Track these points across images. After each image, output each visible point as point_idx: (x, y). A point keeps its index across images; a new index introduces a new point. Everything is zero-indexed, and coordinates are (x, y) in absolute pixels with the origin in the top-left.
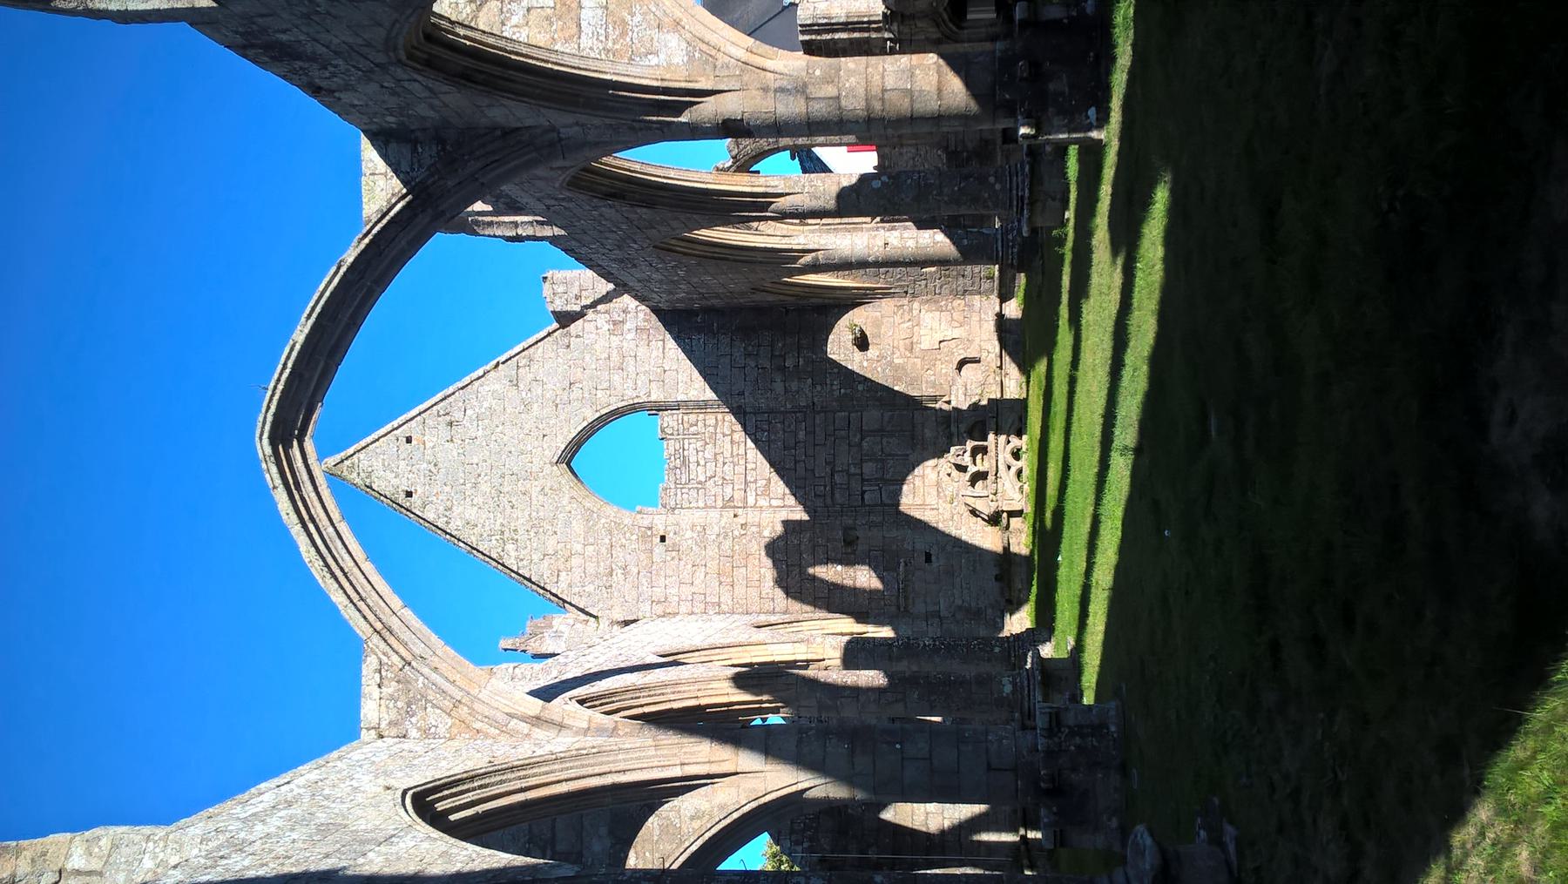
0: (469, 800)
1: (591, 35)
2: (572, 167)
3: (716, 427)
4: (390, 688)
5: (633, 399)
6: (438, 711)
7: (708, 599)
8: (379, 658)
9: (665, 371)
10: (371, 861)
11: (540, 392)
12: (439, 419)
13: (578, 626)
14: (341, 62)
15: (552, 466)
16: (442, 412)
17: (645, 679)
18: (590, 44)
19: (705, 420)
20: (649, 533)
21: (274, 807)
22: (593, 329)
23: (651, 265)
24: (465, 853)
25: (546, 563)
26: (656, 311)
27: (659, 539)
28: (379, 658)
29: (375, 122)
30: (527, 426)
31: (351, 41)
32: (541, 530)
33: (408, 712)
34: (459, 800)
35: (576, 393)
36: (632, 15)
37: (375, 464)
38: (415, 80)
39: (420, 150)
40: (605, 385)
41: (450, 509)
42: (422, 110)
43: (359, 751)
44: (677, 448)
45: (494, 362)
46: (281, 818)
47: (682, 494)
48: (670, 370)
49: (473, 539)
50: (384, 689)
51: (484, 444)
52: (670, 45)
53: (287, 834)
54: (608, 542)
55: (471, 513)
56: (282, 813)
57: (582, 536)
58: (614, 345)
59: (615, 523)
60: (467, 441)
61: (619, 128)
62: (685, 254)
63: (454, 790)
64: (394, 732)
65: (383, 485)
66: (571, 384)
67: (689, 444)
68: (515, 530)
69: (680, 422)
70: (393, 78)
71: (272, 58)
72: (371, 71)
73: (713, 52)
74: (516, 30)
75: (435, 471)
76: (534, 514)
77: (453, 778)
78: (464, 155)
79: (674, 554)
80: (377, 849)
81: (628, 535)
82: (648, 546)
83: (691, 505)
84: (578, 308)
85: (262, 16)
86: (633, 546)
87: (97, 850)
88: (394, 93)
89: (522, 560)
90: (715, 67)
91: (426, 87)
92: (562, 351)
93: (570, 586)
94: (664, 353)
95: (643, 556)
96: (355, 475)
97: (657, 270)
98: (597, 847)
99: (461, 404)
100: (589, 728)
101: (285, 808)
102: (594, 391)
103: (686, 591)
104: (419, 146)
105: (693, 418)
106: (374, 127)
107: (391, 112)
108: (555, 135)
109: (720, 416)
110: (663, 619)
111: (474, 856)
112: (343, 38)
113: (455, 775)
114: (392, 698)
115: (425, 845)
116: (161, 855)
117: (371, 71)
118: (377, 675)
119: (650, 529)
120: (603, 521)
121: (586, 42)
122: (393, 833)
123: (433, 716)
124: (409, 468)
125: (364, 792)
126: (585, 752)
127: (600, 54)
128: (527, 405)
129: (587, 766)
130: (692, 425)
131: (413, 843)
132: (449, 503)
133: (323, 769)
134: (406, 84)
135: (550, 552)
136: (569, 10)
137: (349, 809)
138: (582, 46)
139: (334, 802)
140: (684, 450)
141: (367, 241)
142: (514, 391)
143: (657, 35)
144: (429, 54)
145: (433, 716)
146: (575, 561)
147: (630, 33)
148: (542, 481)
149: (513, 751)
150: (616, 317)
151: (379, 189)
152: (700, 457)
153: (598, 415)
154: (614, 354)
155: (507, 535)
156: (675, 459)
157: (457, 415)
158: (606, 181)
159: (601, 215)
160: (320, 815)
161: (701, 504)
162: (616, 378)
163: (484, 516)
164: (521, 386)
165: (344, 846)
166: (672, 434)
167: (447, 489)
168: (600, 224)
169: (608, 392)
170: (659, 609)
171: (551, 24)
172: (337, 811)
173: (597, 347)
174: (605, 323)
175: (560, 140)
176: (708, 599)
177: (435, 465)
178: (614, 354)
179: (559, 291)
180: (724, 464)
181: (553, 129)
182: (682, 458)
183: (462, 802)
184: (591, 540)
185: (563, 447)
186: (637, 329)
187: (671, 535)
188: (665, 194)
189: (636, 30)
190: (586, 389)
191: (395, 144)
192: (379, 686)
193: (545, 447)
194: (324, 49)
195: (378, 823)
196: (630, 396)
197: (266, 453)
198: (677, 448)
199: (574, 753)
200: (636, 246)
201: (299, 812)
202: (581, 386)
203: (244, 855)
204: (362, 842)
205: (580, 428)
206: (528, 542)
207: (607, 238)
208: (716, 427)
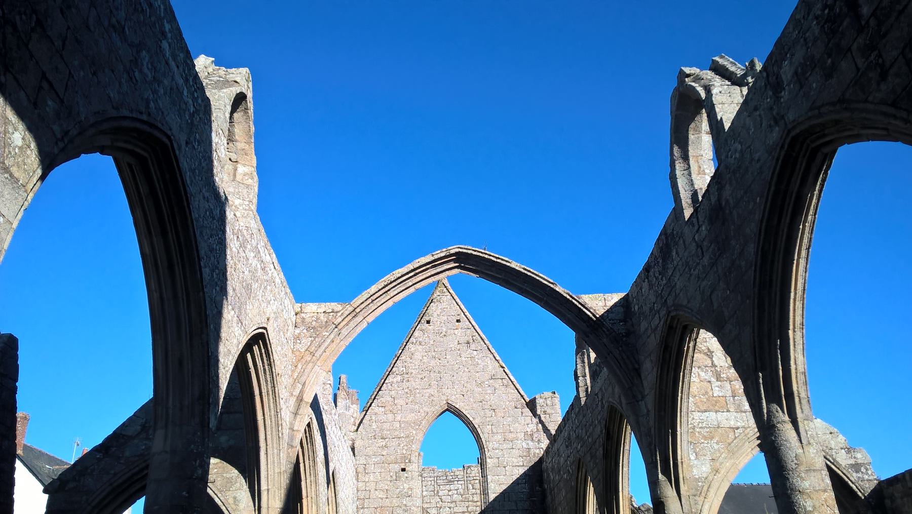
0: (258, 363)
1: (701, 418)
2: (622, 408)
3: (473, 501)
4: (323, 318)
5: (487, 448)
6: (309, 344)
7: (366, 500)
8: (340, 311)
9: (505, 467)
10: (229, 313)
11: (489, 392)
12: (471, 337)
13: (352, 420)
14: (664, 282)
15: (446, 400)
16: (474, 338)
17: (320, 463)
18: (696, 418)
19: (476, 494)
20: (407, 461)
21: (262, 261)
23: (569, 457)
24: (229, 363)
25: (390, 399)
26: (541, 461)
27: (403, 467)
28: (340, 311)
29: (633, 300)
31: (677, 287)
32: (408, 395)
33: (309, 328)
34: (258, 358)
35: (489, 413)
36: (717, 443)
37: (445, 304)
38: (660, 321)
39: (621, 324)
40: (494, 430)
41: (420, 344)
42: (644, 325)
43: (289, 303)
44: (459, 477)
45: (504, 366)
46: (256, 265)
47: (431, 481)
48: (506, 470)
49: (403, 358)
50: (323, 314)
51: (458, 361)
52: (703, 466)
53: (248, 269)
54: (402, 436)
55: (418, 356)
56: (259, 266)
57: (405, 420)
58: (519, 435)
59: (413, 440)
60: (459, 352)
61: (649, 436)
62: (577, 478)
63: (264, 355)
64: (299, 321)
67: (461, 485)
68: (408, 381)
69: (475, 478)
70: (660, 309)
71: (662, 247)
72: (662, 297)
73: (703, 494)
74: (697, 374)
75: (441, 335)
76: (418, 391)
77: (271, 354)
78: (621, 347)
79: (394, 477)
80: (236, 316)
81: (406, 448)
82: (399, 461)
83: (424, 487)
84: (539, 412)
85: (684, 242)
86: (399, 451)
87: (246, 178)
88: (651, 309)
89: (391, 385)
90: (695, 496)
91: (657, 326)
92: (513, 404)
93: (376, 414)
94: (516, 466)
95: (393, 457)
96: (438, 294)
97: (566, 461)
98: (223, 439)
99: (479, 348)
100: (293, 430)
101: (261, 267)
102: (490, 424)
103: (372, 486)
104: (623, 323)
105: (477, 486)
106: (631, 299)
107: (640, 308)
108: (640, 399)
109: (479, 504)
110: (355, 472)
111: (227, 369)
112: (678, 283)
113: (273, 355)
114: (318, 319)
115: (235, 341)
116: (241, 208)
117: (662, 297)
118: (331, 311)
119: (410, 462)
120: (414, 432)
121: (697, 415)
122: (244, 323)
123: (306, 341)
124: (443, 322)
125: (267, 307)
126: (280, 429)
127: (691, 424)
128: (480, 385)
129: (272, 431)
130: (473, 486)
131: (237, 335)
132: (423, 343)
133: (281, 285)
134: (657, 316)
135: (396, 402)
136: (713, 405)
137: (258, 299)
138: (694, 413)
139: (263, 291)
140: (458, 481)
141: (568, 297)
143: (708, 458)
144: (676, 328)
145: (306, 341)
146: (390, 416)
147: (706, 442)
148: (437, 395)
149: (284, 387)
150: (535, 435)
151: (597, 303)
152: (454, 492)
153: (477, 426)
154: (513, 435)
155: (406, 376)
156: (452, 476)
157: (473, 346)
158: (616, 428)
159: (596, 425)
160: (256, 285)
161: (425, 493)
163: (416, 363)
164: (491, 381)
165: (239, 298)
166: (467, 473)
167: (432, 342)
168: (590, 425)
169: (490, 432)
170: (361, 469)
171: (703, 395)
172: (258, 293)
173: (517, 425)
174: (531, 429)
175: (638, 401)
176: (366, 500)
177: (445, 335)
178: (513, 435)
179: (548, 401)
180: (450, 508)
181: (643, 397)
182: (452, 480)
183: (257, 360)
184: (403, 425)
185: (457, 406)
186: (529, 449)
187: (406, 475)
188: (613, 464)
189: (709, 445)
190: (491, 419)
191: (622, 310)
192: (324, 312)
194: (670, 274)
195: (250, 315)
196: (489, 446)
197: (451, 251)
198: (459, 477)
199: (280, 423)
200: (579, 447)
201: (259, 274)
202: (493, 416)
203: (238, 248)
204: (240, 308)
205: (468, 416)
206: (402, 388)
207: (582, 429)
208: (473, 501)
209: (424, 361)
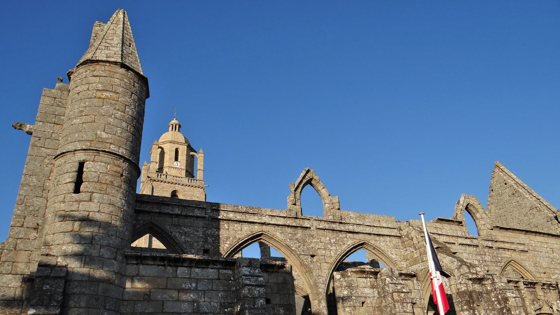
11: (531, 217)
18: (410, 269)
22: (556, 228)
30: (520, 217)
37: (496, 178)
66: (537, 226)
75: (500, 195)
92: (546, 220)
99: (520, 195)
124: (498, 188)
128: (525, 216)
142: (528, 209)
167: (497, 201)
177: (501, 195)
193: (516, 225)
209: (496, 212)
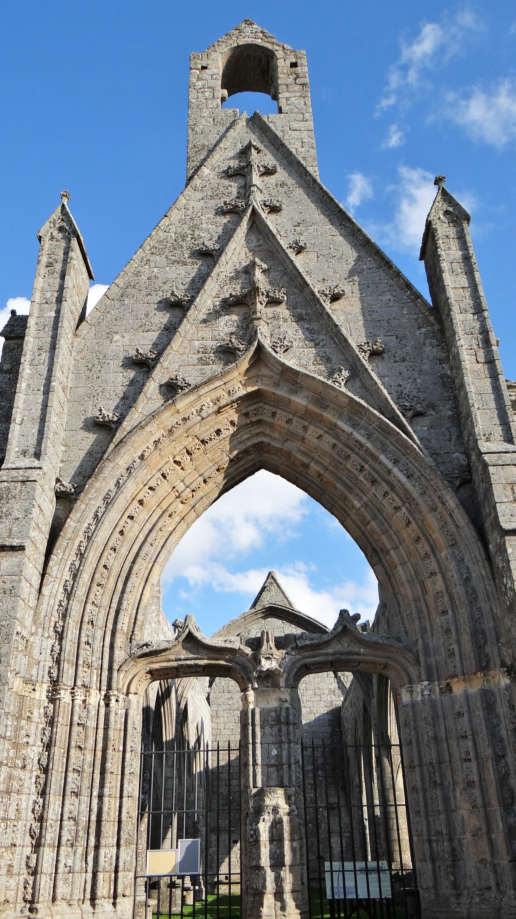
65: (265, 596)
95: (236, 706)
103: (221, 726)
162: (310, 692)
170: (214, 713)
173: (324, 683)
